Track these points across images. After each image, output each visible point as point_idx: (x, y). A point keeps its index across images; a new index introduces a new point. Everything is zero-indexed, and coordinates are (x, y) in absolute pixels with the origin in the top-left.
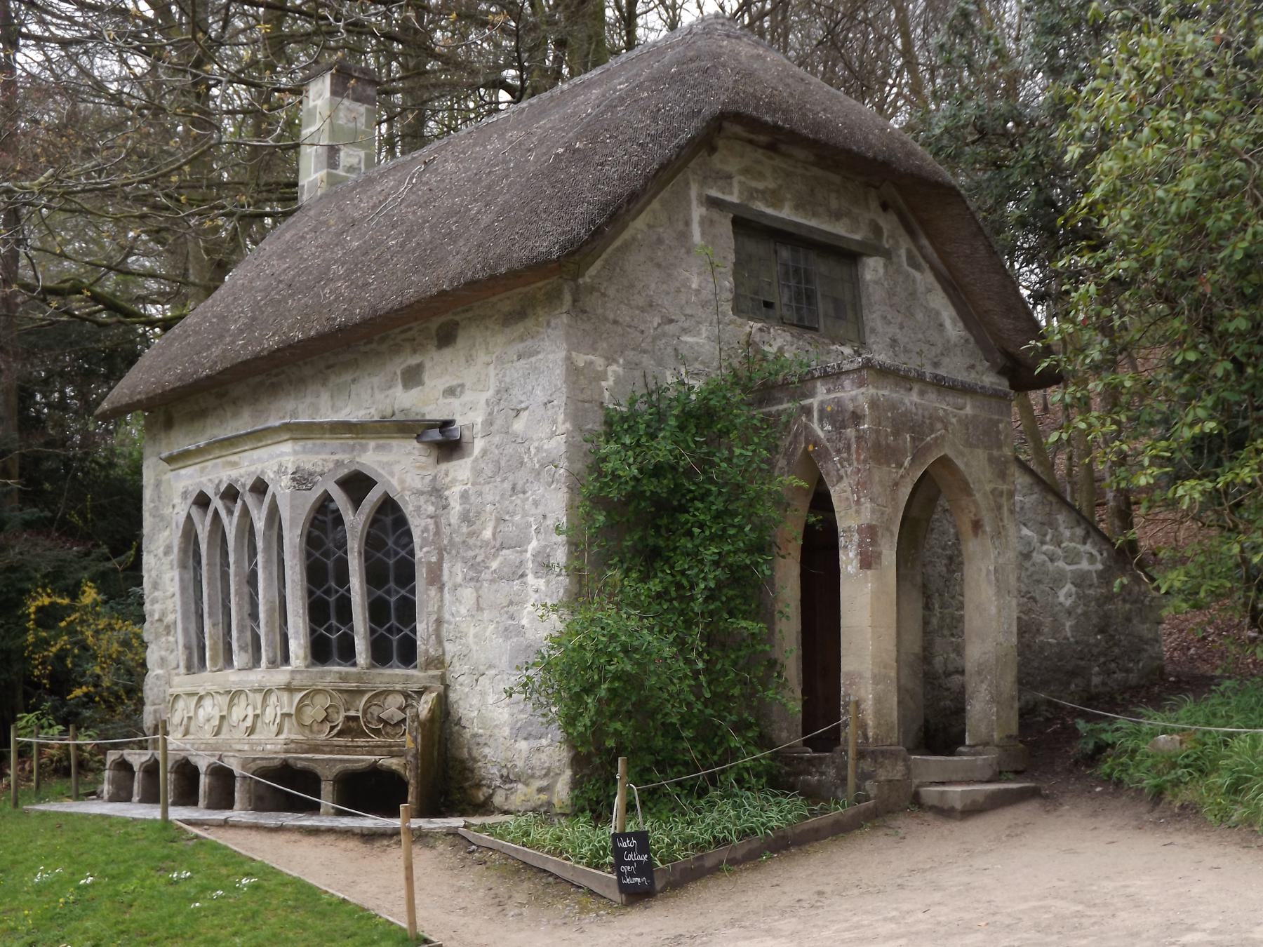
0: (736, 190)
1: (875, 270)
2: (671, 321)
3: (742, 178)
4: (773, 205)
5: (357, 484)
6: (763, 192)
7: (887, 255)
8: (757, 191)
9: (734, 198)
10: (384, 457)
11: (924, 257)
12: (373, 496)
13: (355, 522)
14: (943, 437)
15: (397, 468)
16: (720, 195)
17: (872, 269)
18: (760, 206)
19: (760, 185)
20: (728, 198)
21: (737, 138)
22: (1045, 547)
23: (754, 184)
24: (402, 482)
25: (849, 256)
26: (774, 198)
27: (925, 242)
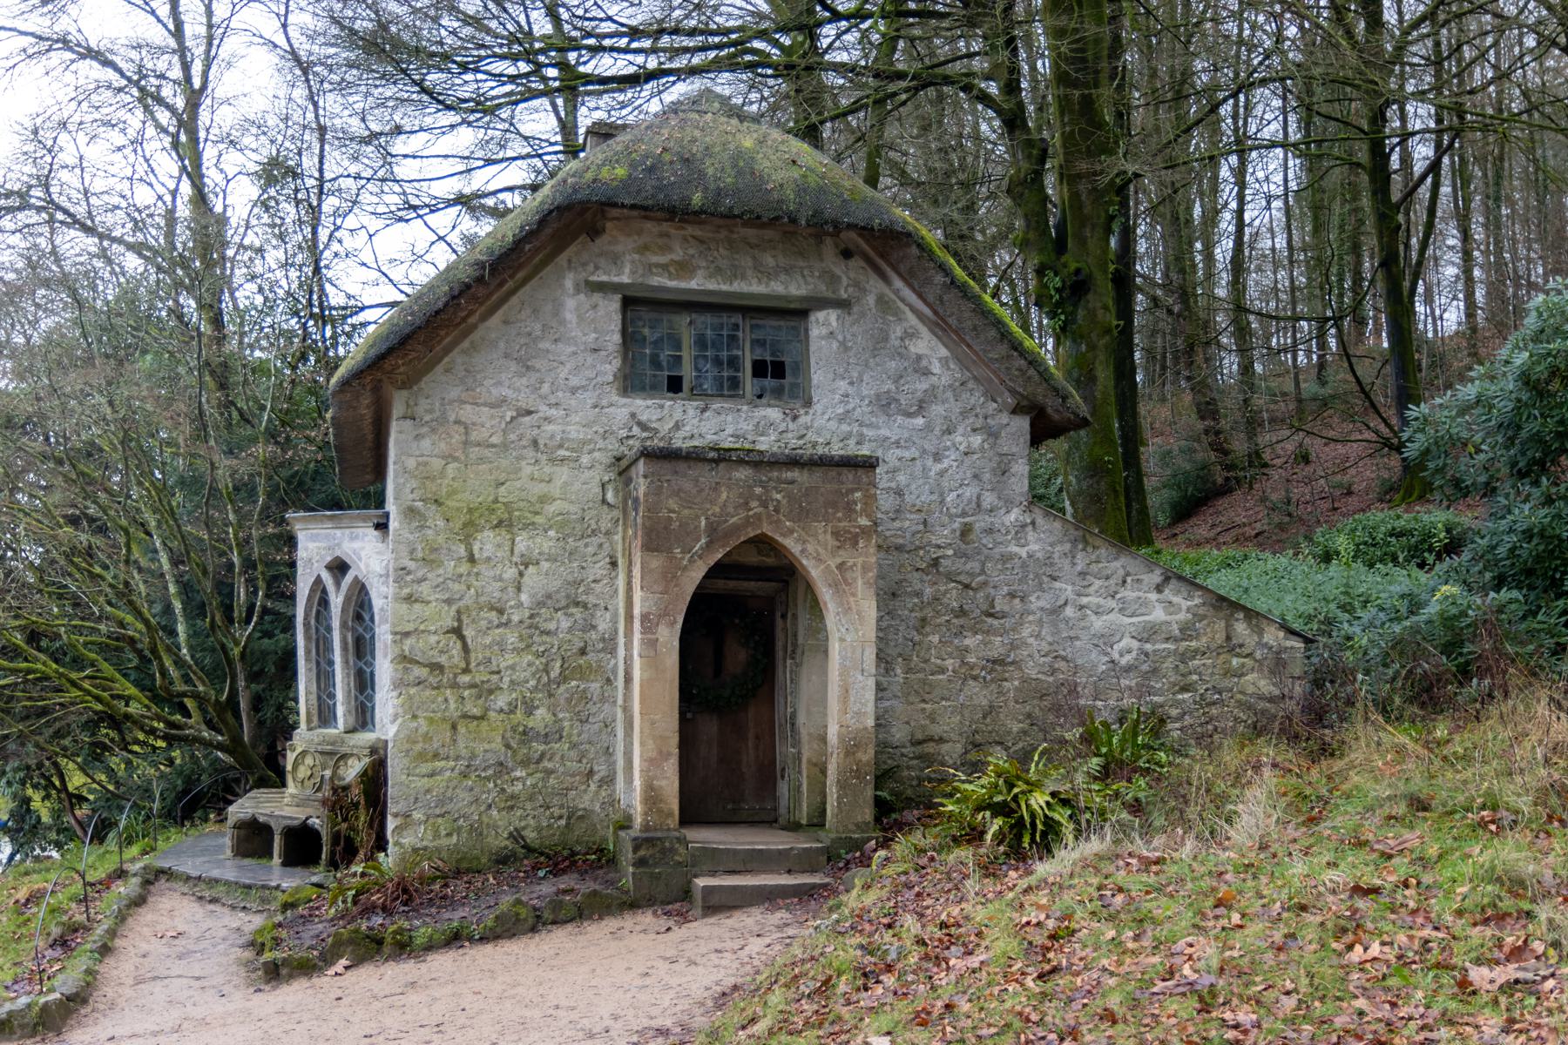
0: (627, 270)
1: (826, 323)
2: (529, 413)
3: (636, 257)
4: (678, 277)
5: (339, 567)
6: (664, 267)
7: (843, 305)
8: (657, 265)
9: (625, 279)
10: (356, 545)
11: (903, 300)
12: (349, 578)
13: (336, 601)
14: (758, 517)
15: (363, 554)
16: (604, 278)
17: (823, 323)
18: (658, 280)
19: (662, 259)
20: (616, 279)
21: (628, 218)
22: (1085, 600)
23: (655, 259)
24: (367, 566)
25: (797, 313)
26: (684, 269)
27: (898, 283)
